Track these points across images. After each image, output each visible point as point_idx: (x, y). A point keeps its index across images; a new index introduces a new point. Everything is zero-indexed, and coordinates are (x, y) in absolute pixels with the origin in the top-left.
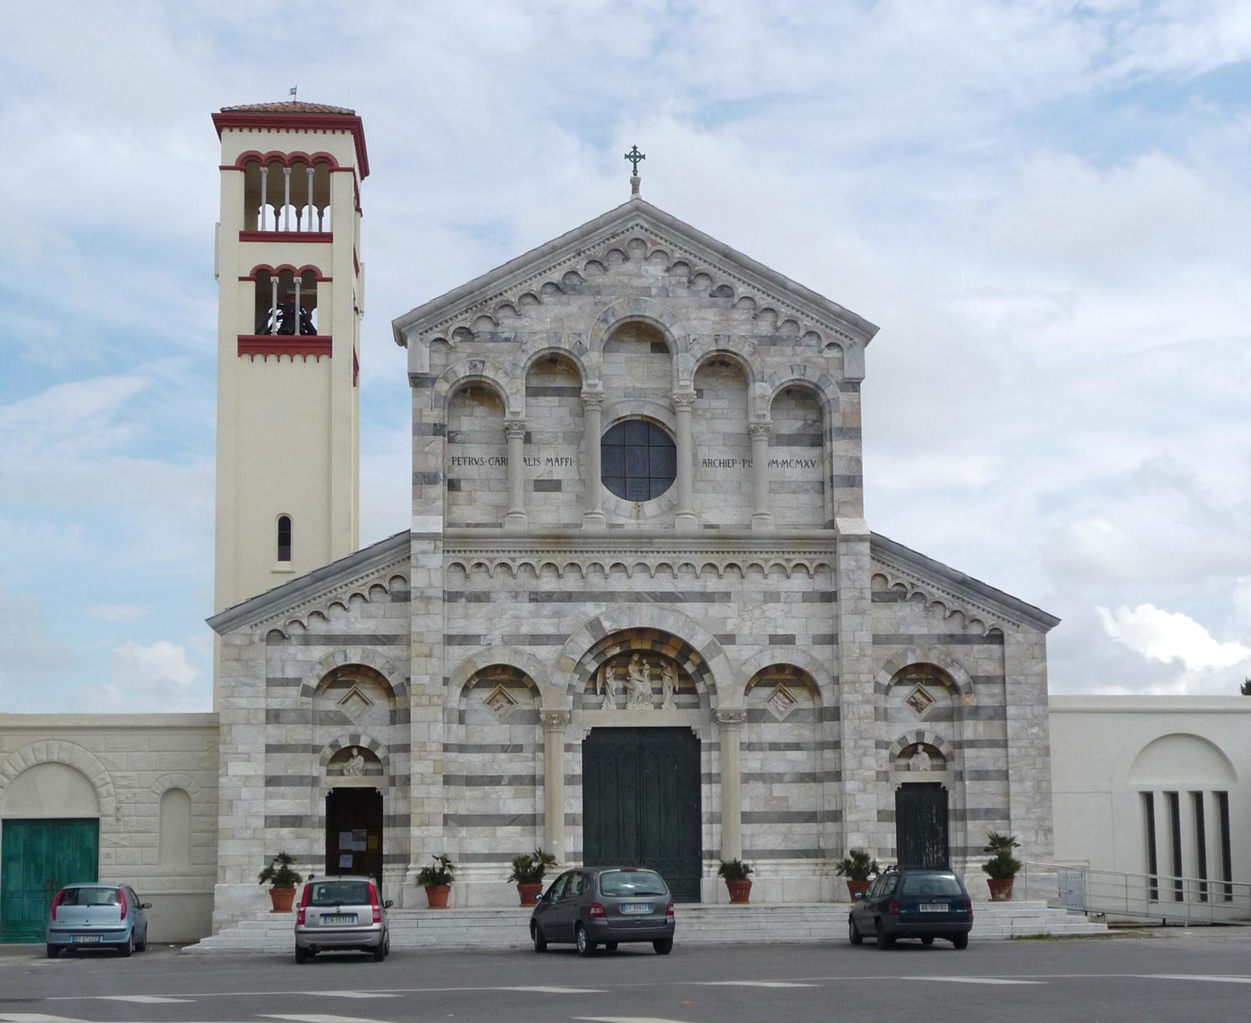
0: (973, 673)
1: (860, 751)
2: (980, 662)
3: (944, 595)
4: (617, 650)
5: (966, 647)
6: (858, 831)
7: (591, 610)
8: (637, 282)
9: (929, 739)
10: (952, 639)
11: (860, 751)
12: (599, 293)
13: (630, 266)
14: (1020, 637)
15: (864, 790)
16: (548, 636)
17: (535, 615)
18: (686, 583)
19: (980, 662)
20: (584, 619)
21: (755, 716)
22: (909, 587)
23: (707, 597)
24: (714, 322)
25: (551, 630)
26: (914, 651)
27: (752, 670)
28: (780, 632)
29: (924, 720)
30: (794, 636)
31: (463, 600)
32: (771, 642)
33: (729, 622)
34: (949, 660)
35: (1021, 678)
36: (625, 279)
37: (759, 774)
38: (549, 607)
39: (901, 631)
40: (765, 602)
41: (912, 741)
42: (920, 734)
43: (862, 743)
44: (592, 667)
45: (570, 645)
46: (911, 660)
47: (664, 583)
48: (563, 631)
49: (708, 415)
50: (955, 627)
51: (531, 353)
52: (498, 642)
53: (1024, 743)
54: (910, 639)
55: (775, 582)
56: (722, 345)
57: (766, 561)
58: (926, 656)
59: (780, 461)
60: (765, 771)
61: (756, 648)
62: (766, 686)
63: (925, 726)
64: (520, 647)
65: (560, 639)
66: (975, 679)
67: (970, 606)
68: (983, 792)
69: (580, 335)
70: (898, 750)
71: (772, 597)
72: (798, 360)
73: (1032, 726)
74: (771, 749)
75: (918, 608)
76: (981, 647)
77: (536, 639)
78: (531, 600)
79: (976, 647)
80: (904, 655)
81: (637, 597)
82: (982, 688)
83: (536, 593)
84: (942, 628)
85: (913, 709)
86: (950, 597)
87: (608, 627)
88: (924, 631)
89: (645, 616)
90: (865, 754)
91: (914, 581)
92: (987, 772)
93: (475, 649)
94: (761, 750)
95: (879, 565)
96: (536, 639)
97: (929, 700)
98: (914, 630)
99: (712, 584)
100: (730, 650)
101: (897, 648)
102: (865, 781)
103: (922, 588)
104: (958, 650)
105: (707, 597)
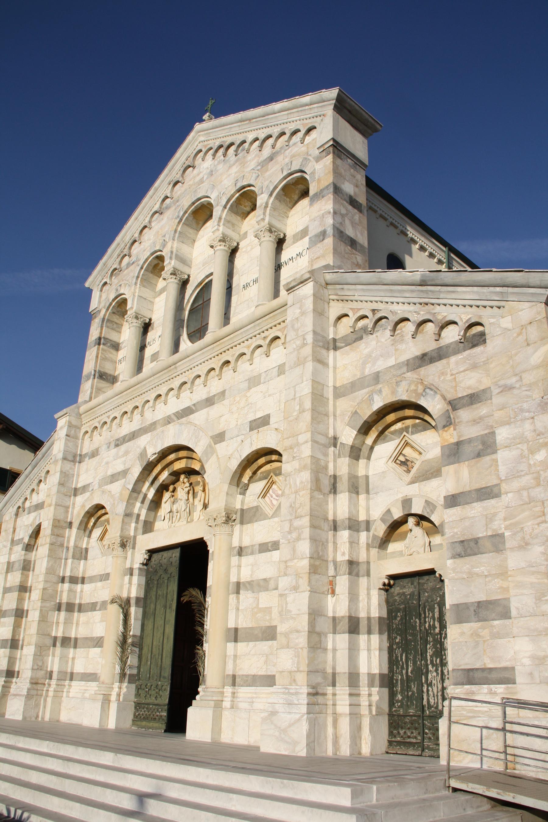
0: (449, 397)
1: (294, 535)
2: (460, 377)
3: (406, 307)
4: (165, 475)
5: (439, 365)
6: (288, 647)
7: (143, 441)
8: (198, 179)
9: (417, 509)
10: (426, 359)
11: (294, 535)
12: (178, 201)
13: (196, 171)
14: (506, 322)
15: (295, 588)
16: (119, 473)
17: (117, 457)
18: (200, 393)
19: (460, 377)
20: (139, 451)
21: (246, 516)
22: (370, 314)
23: (209, 402)
24: (236, 173)
25: (120, 468)
26: (380, 391)
27: (234, 464)
28: (259, 415)
29: (412, 482)
30: (268, 416)
31: (88, 458)
32: (251, 429)
33: (223, 419)
34: (420, 388)
35: (514, 379)
36: (191, 183)
37: (249, 583)
38: (123, 448)
39: (367, 372)
40: (249, 388)
41: (397, 514)
42: (407, 502)
43: (297, 523)
44: (151, 494)
45: (129, 476)
46: (378, 404)
47: (187, 399)
48: (127, 466)
49: (249, 248)
50: (426, 342)
51: (141, 263)
52: (96, 487)
53: (527, 480)
54: (377, 378)
55: (261, 363)
56: (239, 185)
57: (248, 347)
58: (394, 392)
59: (294, 256)
60: (255, 578)
61: (239, 439)
62: (260, 479)
63: (412, 490)
64: (106, 487)
65: (124, 473)
66: (454, 405)
67: (438, 309)
68: (471, 575)
69: (164, 236)
70: (380, 529)
71: (254, 381)
72: (287, 160)
73: (532, 452)
74: (260, 552)
75: (384, 334)
76: (460, 357)
77: (114, 478)
78: (117, 445)
79: (453, 359)
80: (371, 399)
81: (168, 421)
82: (464, 414)
83: (118, 440)
84: (412, 349)
85: (400, 470)
86: (412, 308)
87: (152, 453)
88: (392, 362)
89: (171, 437)
90: (298, 539)
91: (375, 306)
92: (476, 541)
93: (87, 494)
94: (252, 553)
95: (341, 304)
96: (114, 478)
97: (420, 453)
98: (381, 365)
99: (215, 386)
100: (220, 448)
101: (362, 393)
102: (298, 575)
103: (384, 310)
104: (431, 372)
105: (209, 402)
